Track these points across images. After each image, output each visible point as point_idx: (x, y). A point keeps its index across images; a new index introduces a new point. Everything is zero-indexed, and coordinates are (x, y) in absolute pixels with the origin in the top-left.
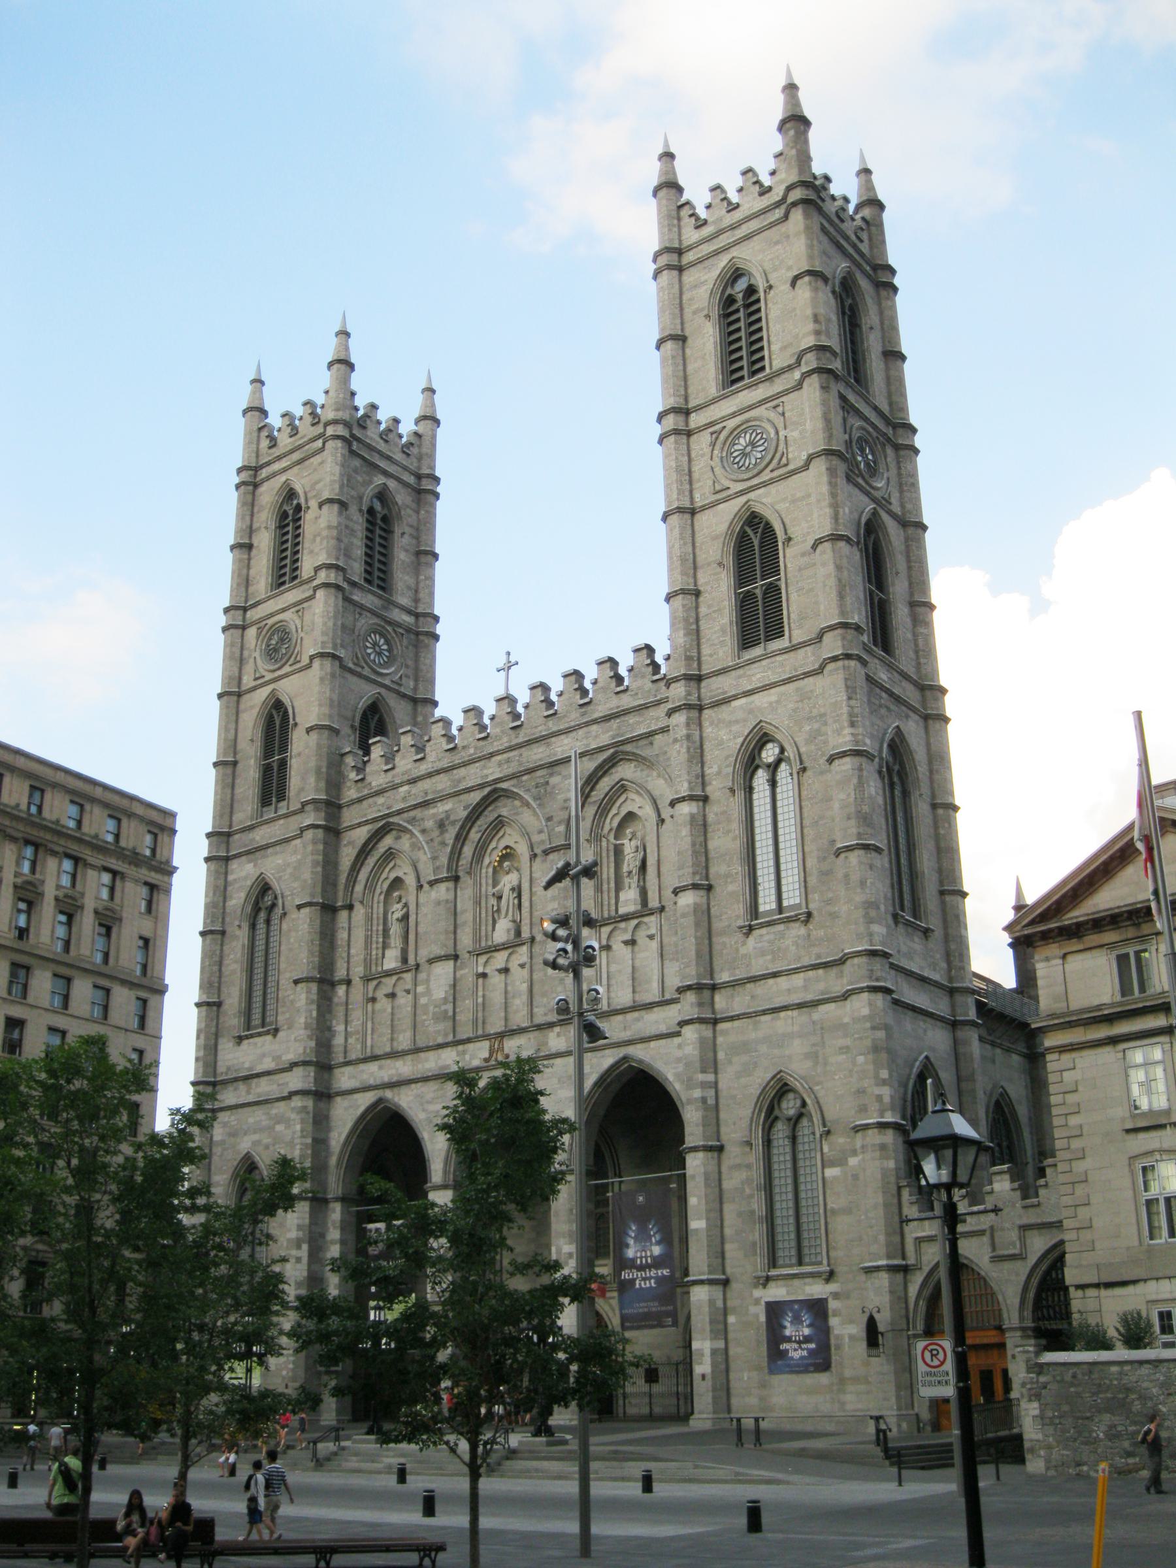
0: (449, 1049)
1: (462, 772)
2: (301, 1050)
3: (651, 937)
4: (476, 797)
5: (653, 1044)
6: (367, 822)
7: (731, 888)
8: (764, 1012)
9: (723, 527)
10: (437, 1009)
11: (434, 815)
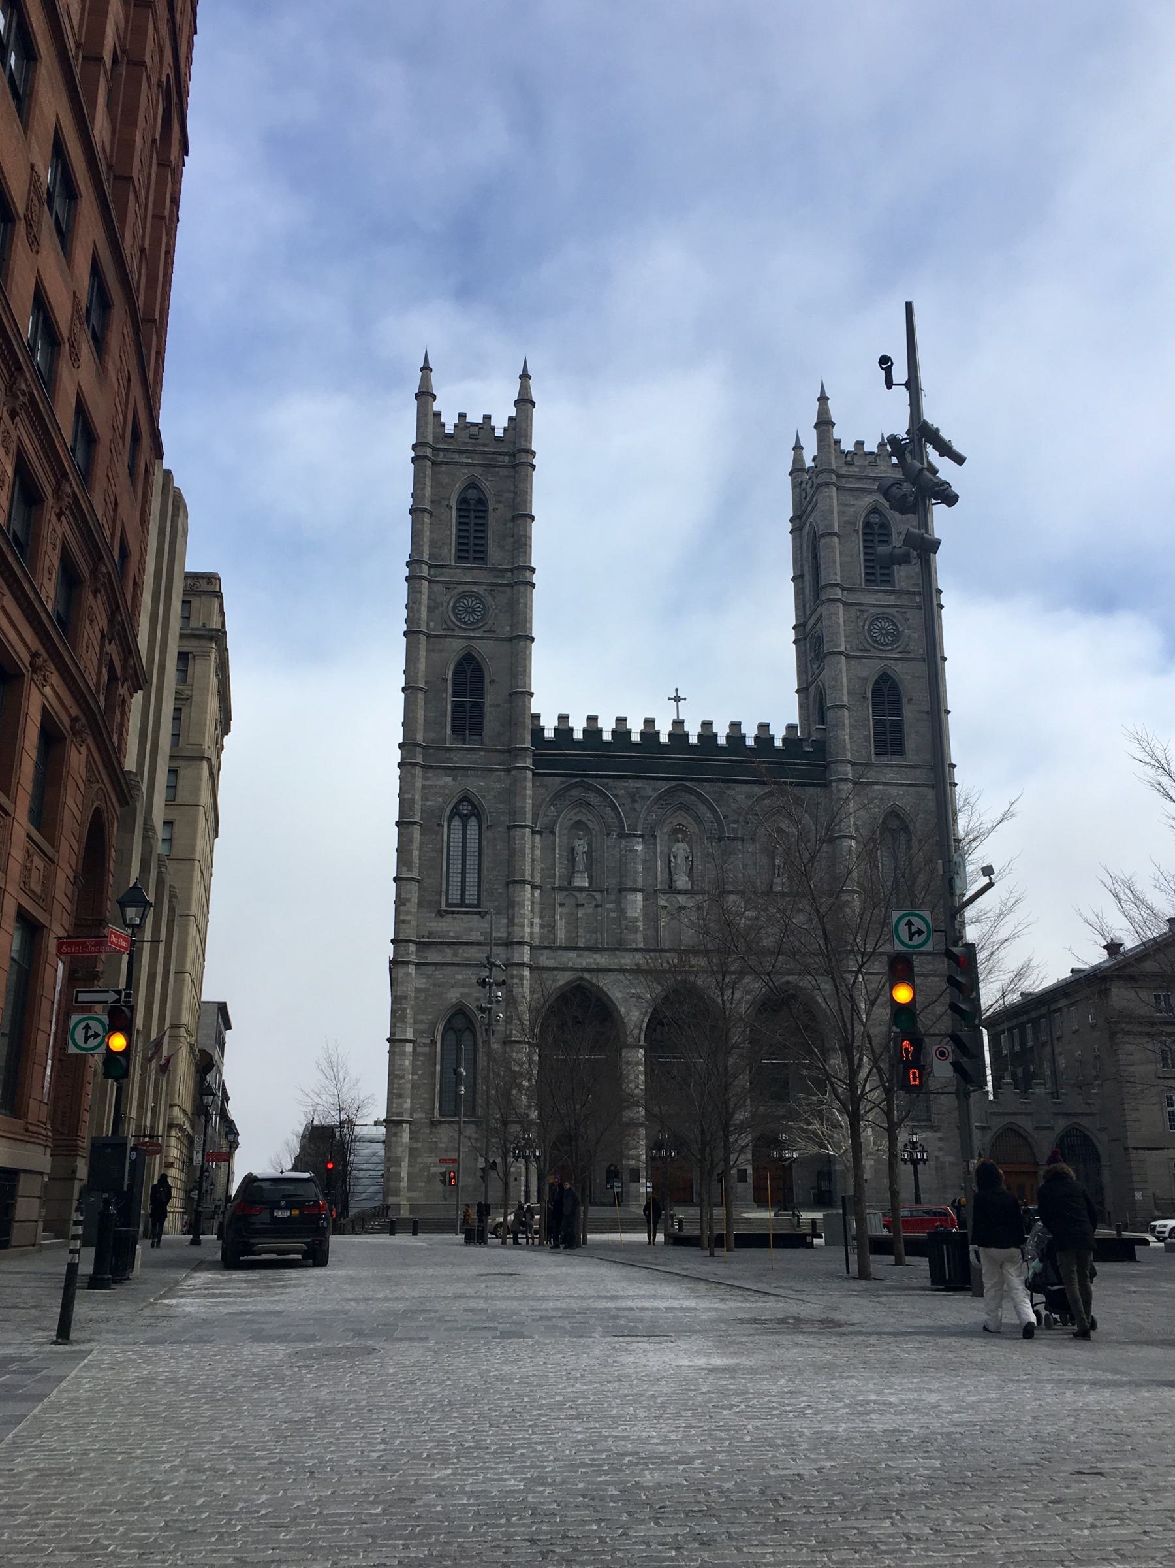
11: (625, 788)
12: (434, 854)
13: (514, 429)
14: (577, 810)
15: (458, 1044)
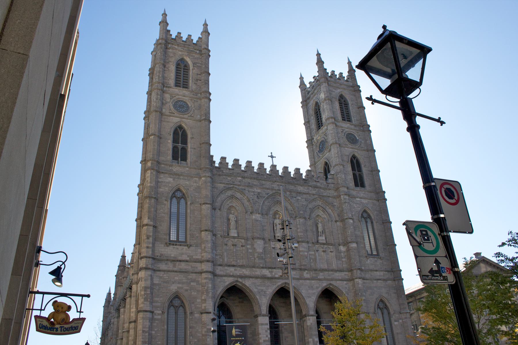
0: (266, 269)
1: (264, 182)
2: (210, 257)
3: (331, 252)
4: (271, 192)
5: (338, 282)
6: (224, 183)
7: (362, 245)
8: (375, 280)
9: (347, 154)
10: (259, 255)
11: (253, 192)
12: (163, 215)
13: (201, 42)
14: (231, 201)
15: (176, 313)
